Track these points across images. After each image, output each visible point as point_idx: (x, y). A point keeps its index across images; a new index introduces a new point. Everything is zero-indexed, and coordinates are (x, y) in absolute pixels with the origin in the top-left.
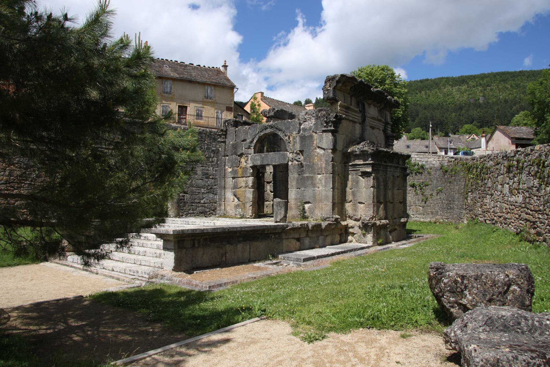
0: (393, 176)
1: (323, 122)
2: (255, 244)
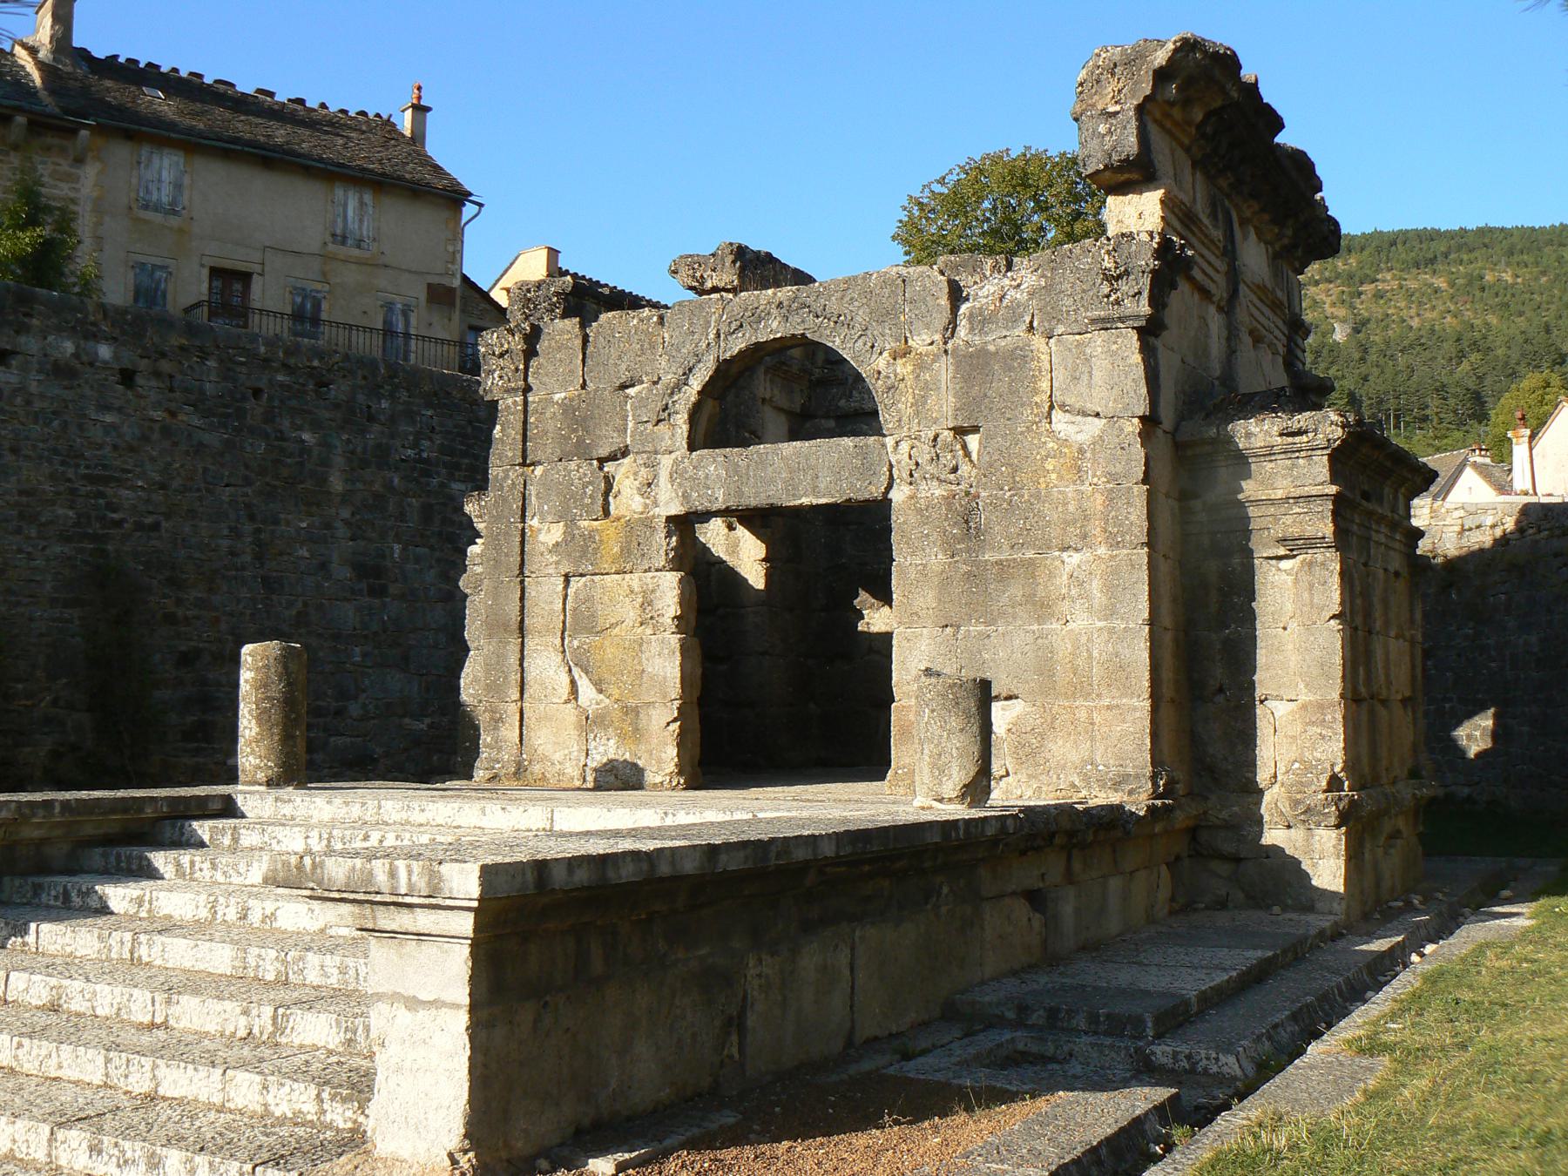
0: (1386, 570)
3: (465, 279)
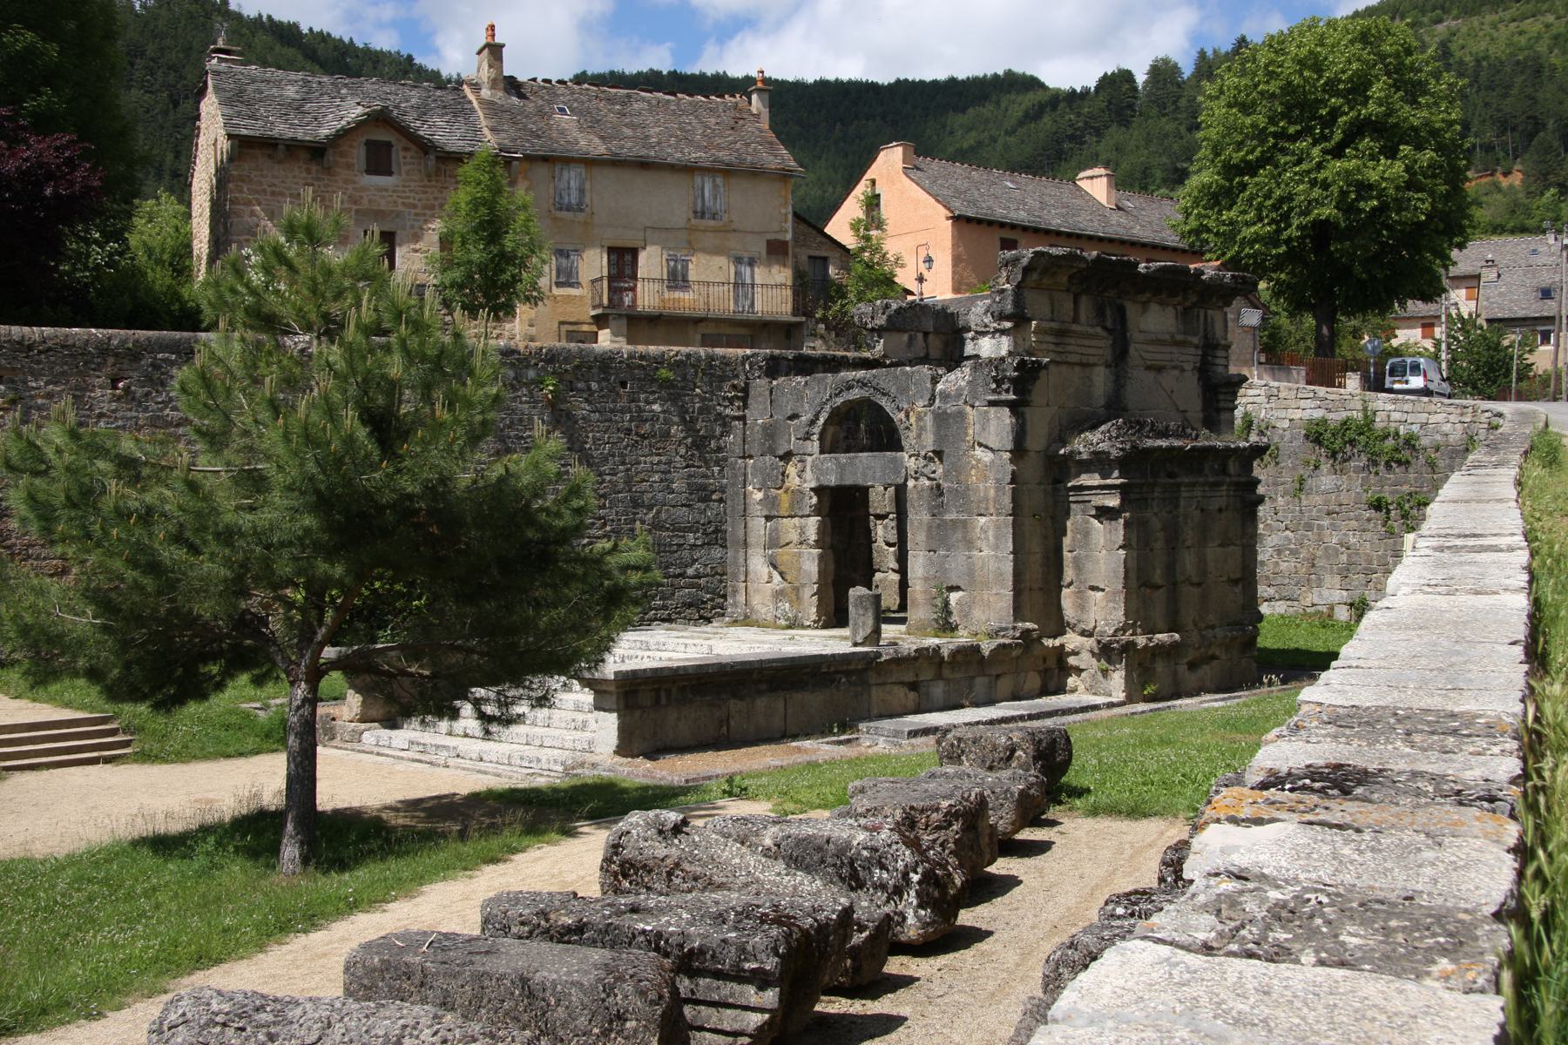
1: (989, 379)
2: (798, 696)
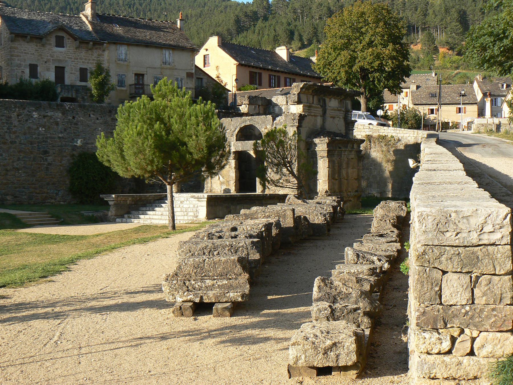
3: (196, 66)
